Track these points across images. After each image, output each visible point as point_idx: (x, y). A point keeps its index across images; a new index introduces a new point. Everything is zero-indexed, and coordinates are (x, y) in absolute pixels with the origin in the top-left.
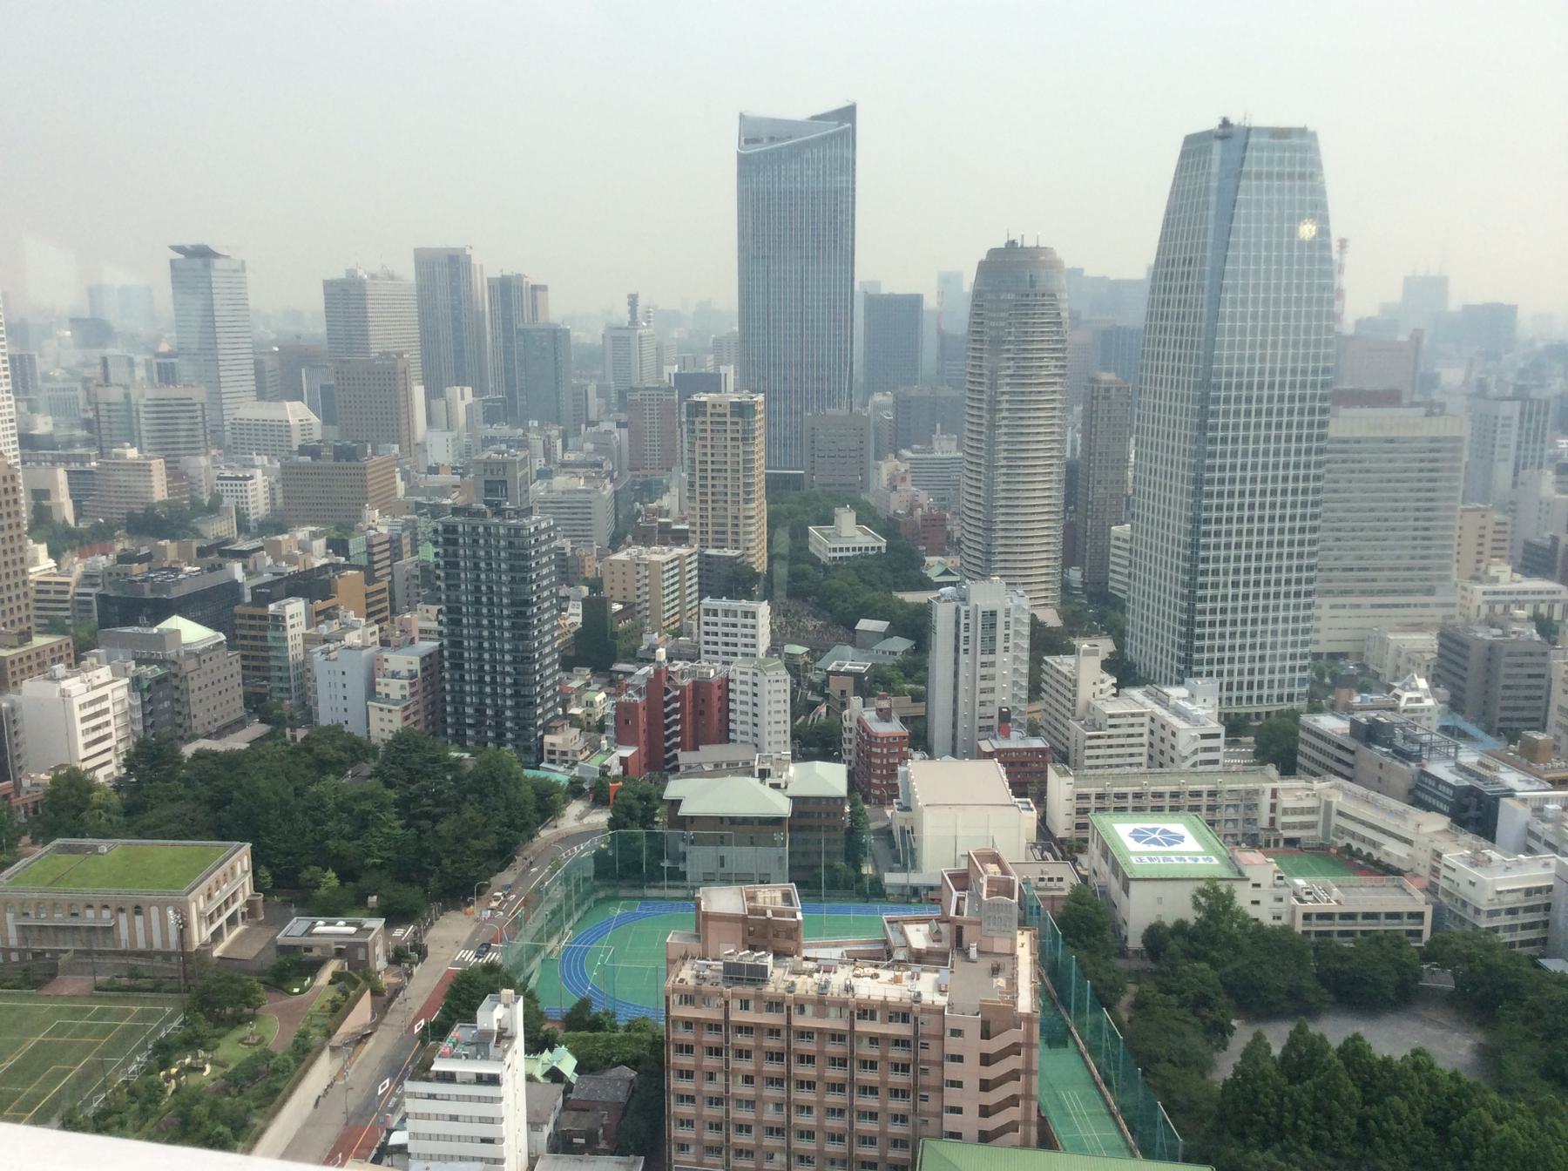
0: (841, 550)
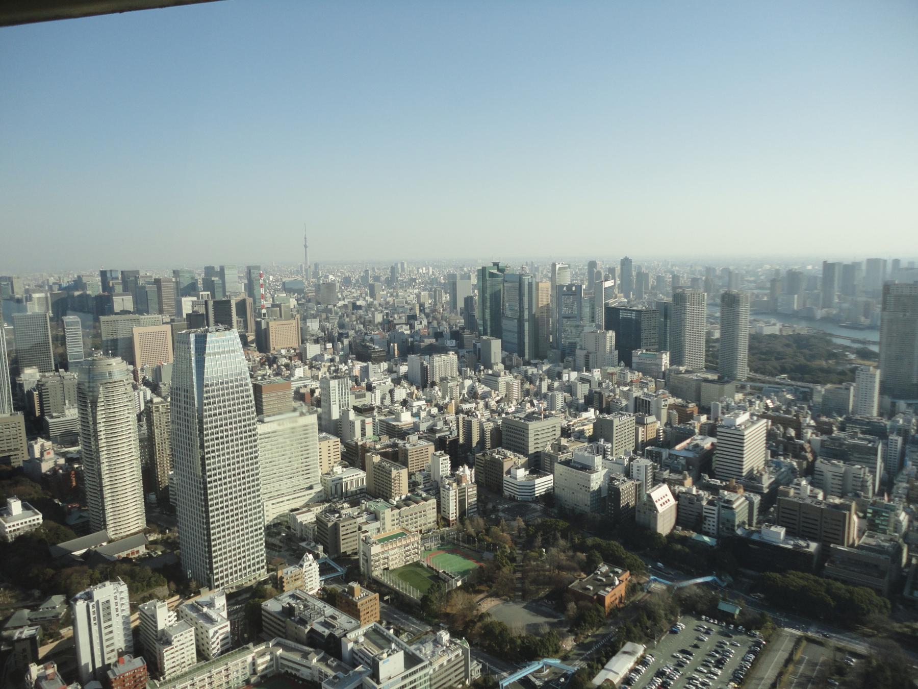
0: (14, 526)
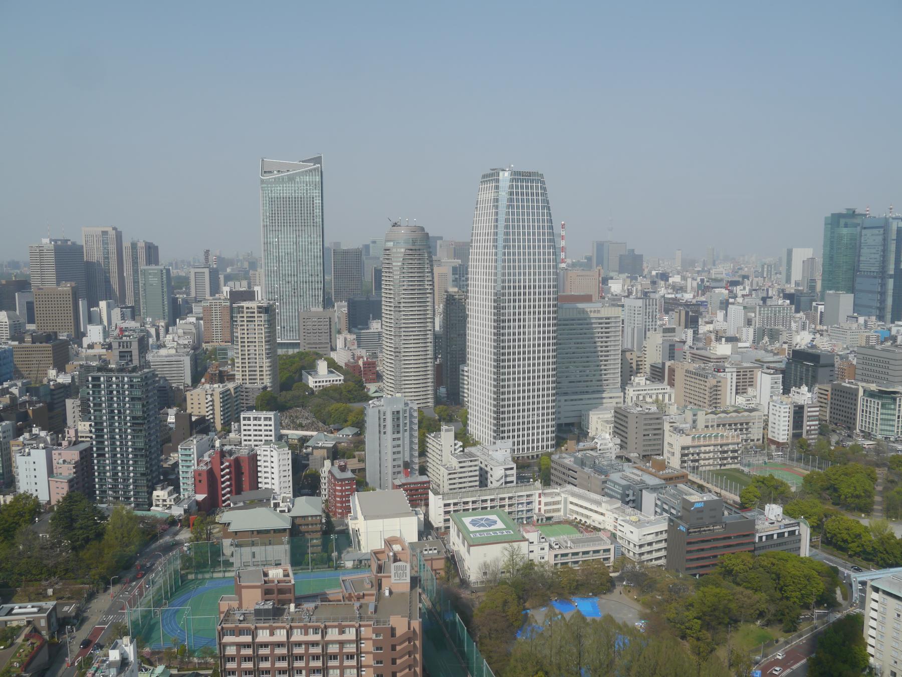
0: (319, 382)
